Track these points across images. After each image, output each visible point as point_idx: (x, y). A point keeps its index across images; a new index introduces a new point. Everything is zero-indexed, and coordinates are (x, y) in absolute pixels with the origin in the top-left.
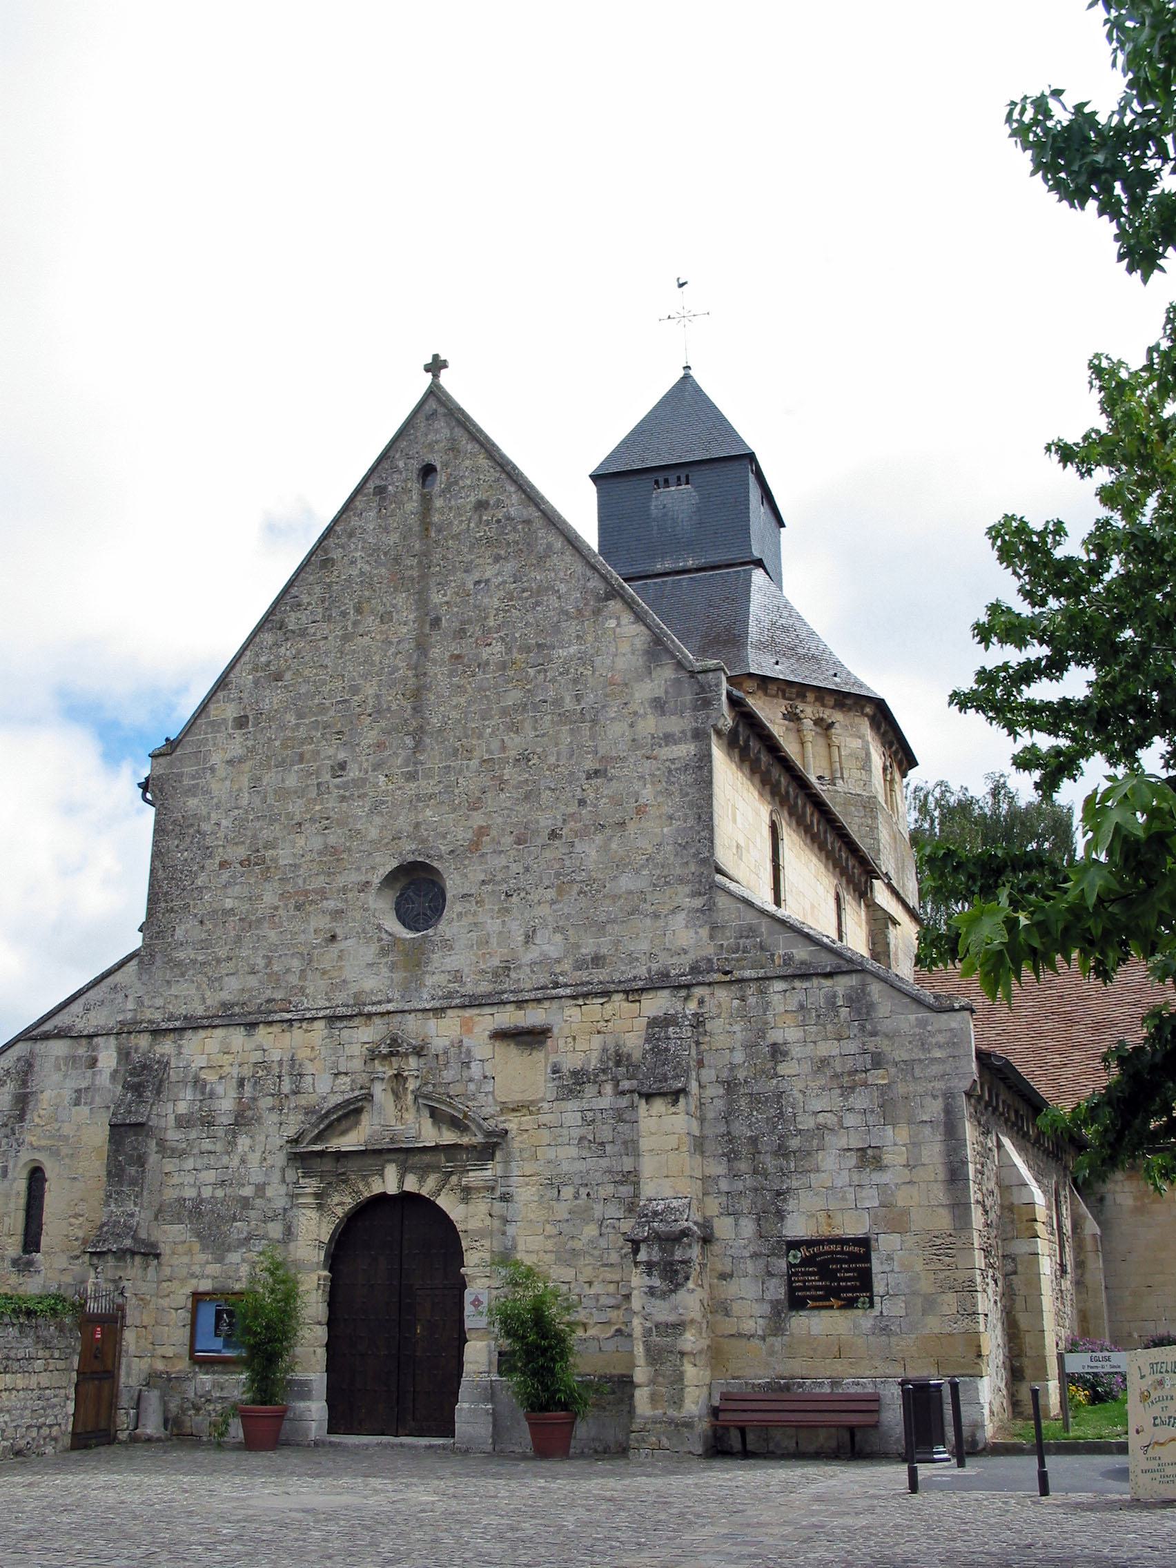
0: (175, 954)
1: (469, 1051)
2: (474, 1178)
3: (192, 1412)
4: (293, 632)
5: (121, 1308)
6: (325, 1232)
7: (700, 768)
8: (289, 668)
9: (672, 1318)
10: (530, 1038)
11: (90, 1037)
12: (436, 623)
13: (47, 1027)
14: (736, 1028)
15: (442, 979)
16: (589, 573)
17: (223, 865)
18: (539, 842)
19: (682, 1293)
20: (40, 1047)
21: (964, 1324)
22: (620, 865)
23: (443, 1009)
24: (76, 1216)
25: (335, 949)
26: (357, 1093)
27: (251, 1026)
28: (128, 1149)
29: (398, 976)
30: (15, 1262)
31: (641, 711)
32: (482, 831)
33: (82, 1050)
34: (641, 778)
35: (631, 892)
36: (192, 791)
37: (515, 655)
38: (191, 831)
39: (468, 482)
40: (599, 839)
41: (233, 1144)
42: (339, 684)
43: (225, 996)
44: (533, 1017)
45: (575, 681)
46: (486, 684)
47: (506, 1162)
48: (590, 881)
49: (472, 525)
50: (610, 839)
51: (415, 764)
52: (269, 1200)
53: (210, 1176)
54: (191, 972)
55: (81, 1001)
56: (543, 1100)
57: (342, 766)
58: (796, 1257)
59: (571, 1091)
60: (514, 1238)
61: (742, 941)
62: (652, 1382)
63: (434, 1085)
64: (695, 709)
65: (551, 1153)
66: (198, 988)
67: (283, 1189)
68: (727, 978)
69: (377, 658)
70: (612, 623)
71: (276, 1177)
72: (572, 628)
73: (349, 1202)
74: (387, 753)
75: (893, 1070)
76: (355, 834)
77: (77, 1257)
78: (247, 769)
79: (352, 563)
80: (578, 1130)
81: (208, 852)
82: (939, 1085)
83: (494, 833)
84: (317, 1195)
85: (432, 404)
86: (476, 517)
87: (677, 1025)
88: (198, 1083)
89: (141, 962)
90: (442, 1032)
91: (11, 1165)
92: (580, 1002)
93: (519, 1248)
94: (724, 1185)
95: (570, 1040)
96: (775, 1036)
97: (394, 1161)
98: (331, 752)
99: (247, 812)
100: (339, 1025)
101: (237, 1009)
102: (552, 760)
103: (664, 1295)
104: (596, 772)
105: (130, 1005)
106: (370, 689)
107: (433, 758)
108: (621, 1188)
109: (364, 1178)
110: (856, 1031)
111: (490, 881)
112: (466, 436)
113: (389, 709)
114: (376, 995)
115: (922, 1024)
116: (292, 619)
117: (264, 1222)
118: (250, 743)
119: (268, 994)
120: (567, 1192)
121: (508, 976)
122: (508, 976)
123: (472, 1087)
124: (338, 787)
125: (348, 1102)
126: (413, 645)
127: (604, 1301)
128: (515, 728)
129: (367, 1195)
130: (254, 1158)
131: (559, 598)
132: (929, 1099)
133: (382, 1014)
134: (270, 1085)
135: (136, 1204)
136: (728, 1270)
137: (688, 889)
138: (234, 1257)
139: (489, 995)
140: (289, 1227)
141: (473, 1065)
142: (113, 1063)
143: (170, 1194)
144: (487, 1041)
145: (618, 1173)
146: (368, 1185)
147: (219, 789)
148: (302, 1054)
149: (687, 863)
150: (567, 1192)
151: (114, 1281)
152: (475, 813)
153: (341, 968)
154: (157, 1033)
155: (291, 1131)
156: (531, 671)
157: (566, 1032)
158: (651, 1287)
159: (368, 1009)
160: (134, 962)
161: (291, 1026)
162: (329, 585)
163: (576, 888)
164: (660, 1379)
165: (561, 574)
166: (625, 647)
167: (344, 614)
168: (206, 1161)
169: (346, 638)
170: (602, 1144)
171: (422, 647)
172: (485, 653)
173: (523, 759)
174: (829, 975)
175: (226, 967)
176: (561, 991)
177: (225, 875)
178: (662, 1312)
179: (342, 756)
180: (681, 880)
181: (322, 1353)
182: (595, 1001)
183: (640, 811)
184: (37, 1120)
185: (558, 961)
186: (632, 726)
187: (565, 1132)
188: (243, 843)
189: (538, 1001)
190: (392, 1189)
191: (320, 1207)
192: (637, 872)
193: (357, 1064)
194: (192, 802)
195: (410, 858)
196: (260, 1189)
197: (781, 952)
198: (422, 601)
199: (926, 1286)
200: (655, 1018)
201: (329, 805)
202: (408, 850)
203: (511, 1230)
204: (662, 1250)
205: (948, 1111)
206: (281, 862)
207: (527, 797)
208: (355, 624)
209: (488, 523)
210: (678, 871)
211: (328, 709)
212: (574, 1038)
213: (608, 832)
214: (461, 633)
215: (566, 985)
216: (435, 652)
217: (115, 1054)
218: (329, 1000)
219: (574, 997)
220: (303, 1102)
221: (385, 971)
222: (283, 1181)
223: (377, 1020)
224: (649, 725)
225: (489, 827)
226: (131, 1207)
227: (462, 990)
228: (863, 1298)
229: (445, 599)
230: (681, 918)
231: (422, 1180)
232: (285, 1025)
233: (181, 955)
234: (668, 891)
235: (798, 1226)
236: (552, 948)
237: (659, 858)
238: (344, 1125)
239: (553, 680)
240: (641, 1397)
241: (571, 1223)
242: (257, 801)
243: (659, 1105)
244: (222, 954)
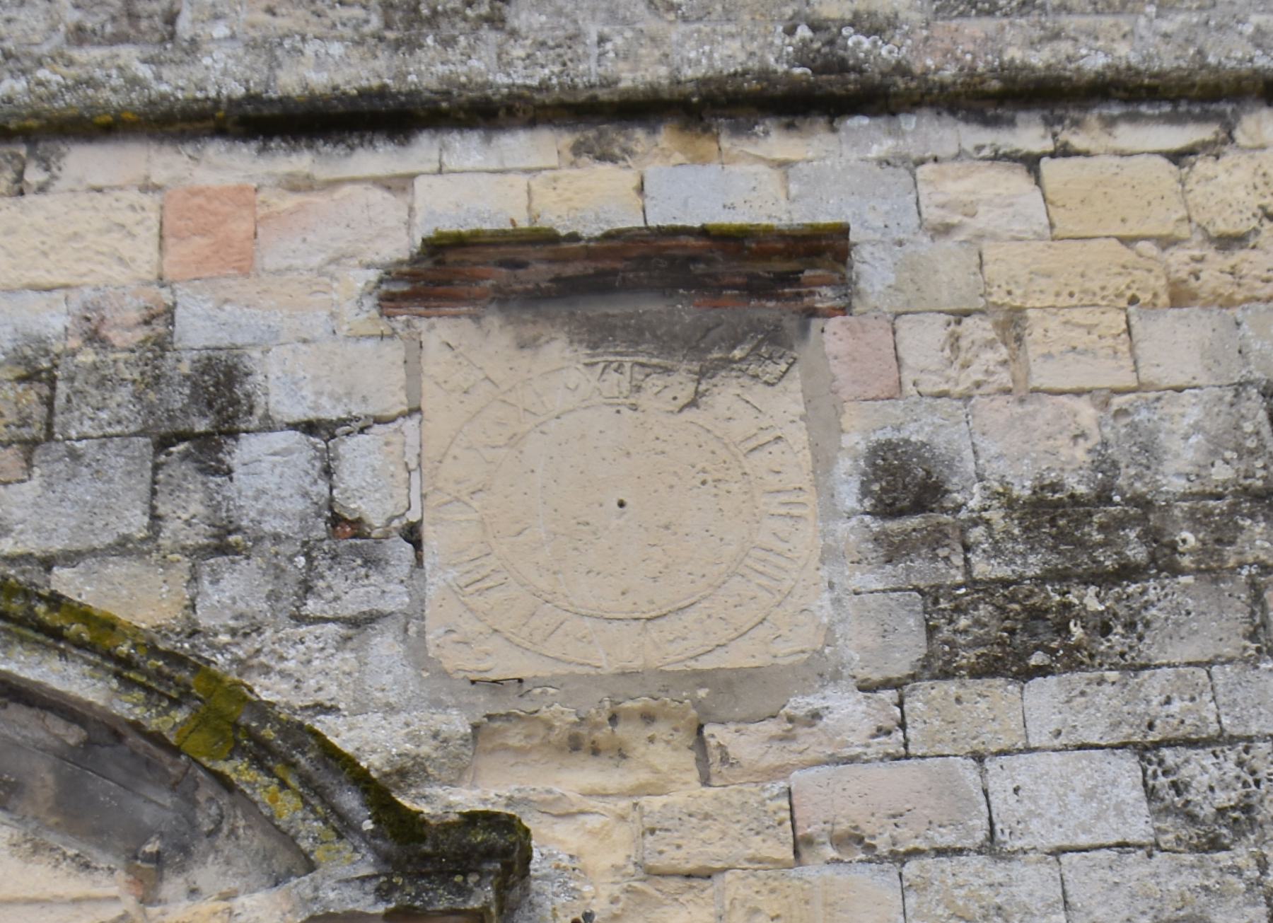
56: (821, 671)
80: (1136, 867)
92: (1029, 135)
144: (365, 316)
182: (1128, 136)
212: (1012, 324)
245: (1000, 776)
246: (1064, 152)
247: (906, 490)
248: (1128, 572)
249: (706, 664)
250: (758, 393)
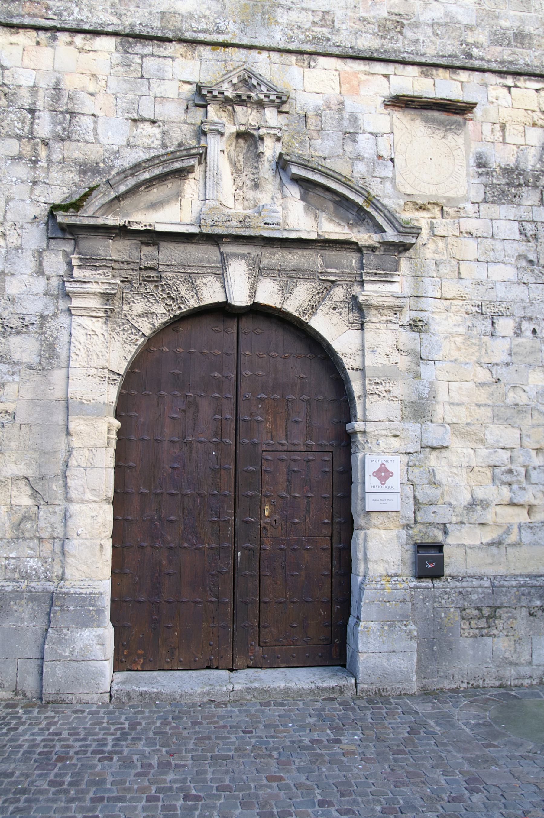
1: (354, 119)
2: (371, 292)
6: (119, 355)
15: (306, 19)
52: (12, 300)
56: (465, 199)
60: (431, 383)
67: (39, 285)
71: (26, 263)
73: (162, 313)
80: (515, 245)
84: (107, 297)
92: (509, 81)
93: (439, 398)
95: (497, 127)
97: (243, 256)
100: (139, 48)
109: (190, 279)
114: (198, 21)
120: (506, 325)
121: (401, 32)
122: (401, 32)
129: (193, 304)
140: (51, 347)
141: (361, 138)
146: (195, 289)
148: (70, 83)
150: (506, 325)
157: (493, 116)
161: (54, 38)
185: (469, 28)
190: (240, 298)
191: (109, 315)
193: (173, 111)
203: (426, 371)
212: (503, 127)
218: (119, 16)
220: (77, 155)
222: (40, 271)
227: (335, 39)
231: (286, 290)
236: (461, 11)
241: (512, 368)
245: (496, 223)
246: (516, 86)
247: (481, 163)
248: (520, 185)
249: (446, 195)
250: (456, 137)
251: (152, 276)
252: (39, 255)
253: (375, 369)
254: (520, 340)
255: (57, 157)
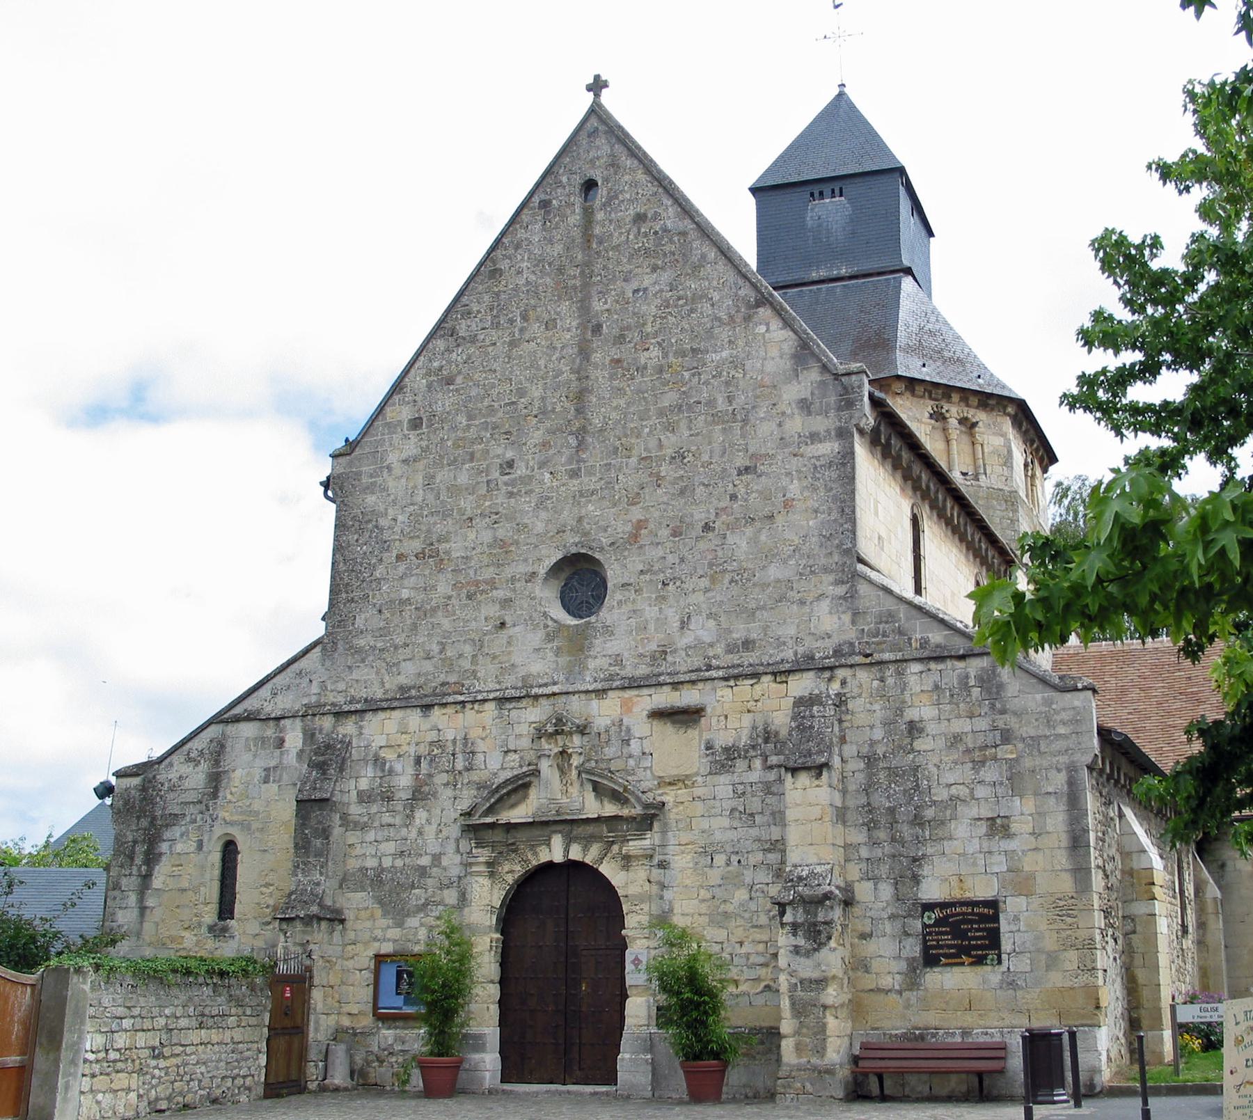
0: (355, 641)
1: (628, 730)
2: (634, 847)
3: (376, 1064)
4: (464, 338)
5: (309, 969)
6: (496, 897)
7: (843, 464)
8: (460, 373)
9: (816, 975)
10: (686, 716)
11: (277, 719)
12: (597, 329)
13: (238, 710)
14: (877, 707)
15: (602, 662)
16: (741, 282)
17: (400, 557)
18: (694, 534)
19: (824, 951)
20: (231, 729)
21: (1084, 979)
22: (770, 556)
23: (604, 691)
24: (267, 885)
25: (504, 634)
26: (525, 769)
27: (427, 708)
28: (313, 822)
29: (564, 660)
30: (211, 929)
31: (789, 412)
32: (640, 525)
33: (270, 731)
34: (788, 474)
35: (778, 581)
36: (370, 489)
37: (672, 359)
38: (370, 526)
39: (628, 196)
40: (749, 531)
41: (410, 817)
42: (507, 387)
43: (402, 680)
44: (688, 697)
45: (727, 383)
46: (643, 387)
47: (664, 833)
48: (741, 571)
49: (631, 237)
50: (760, 530)
51: (578, 462)
52: (445, 869)
53: (390, 847)
54: (371, 658)
55: (269, 686)
56: (697, 774)
57: (510, 464)
58: (931, 917)
59: (723, 766)
61: (881, 626)
62: (797, 1033)
63: (597, 762)
64: (839, 409)
65: (705, 824)
66: (377, 673)
67: (457, 859)
68: (868, 660)
69: (542, 363)
70: (762, 329)
71: (451, 848)
72: (724, 334)
74: (551, 452)
75: (1020, 746)
76: (522, 528)
77: (269, 923)
78: (421, 467)
79: (519, 273)
81: (385, 545)
82: (1063, 759)
83: (651, 526)
84: (489, 864)
85: (594, 122)
86: (635, 229)
87: (821, 704)
88: (378, 762)
89: (324, 649)
90: (603, 712)
91: (206, 838)
92: (732, 683)
94: (864, 853)
95: (722, 718)
96: (912, 714)
98: (499, 451)
99: (421, 508)
100: (508, 706)
101: (413, 692)
102: (705, 458)
103: (808, 954)
104: (747, 468)
105: (315, 689)
106: (536, 392)
107: (594, 456)
108: (769, 855)
109: (533, 847)
110: (986, 709)
111: (648, 571)
112: (626, 152)
113: (553, 410)
115: (1048, 702)
116: (463, 326)
117: (441, 889)
118: (424, 444)
119: (442, 678)
123: (631, 762)
124: (506, 484)
125: (517, 777)
126: (576, 350)
127: (753, 959)
128: (671, 428)
129: (535, 863)
130: (430, 831)
131: (713, 305)
132: (1054, 772)
133: (548, 696)
134: (444, 763)
135: (321, 874)
136: (868, 930)
137: (831, 578)
138: (413, 922)
139: (648, 677)
140: (464, 894)
141: (632, 742)
142: (300, 744)
143: (353, 864)
144: (645, 719)
145: (766, 842)
146: (536, 854)
147: (396, 486)
148: (474, 734)
149: (831, 554)
150: (720, 859)
151: (302, 945)
152: (634, 508)
153: (509, 653)
154: (339, 715)
155: (465, 805)
156: (687, 375)
158: (796, 946)
159: (535, 691)
160: (318, 649)
161: (464, 707)
162: (498, 294)
163: (728, 577)
164: (804, 1030)
165: (715, 283)
166: (774, 352)
167: (511, 321)
168: (386, 833)
169: (513, 344)
170: (752, 815)
171: (584, 352)
172: (643, 358)
173: (679, 456)
174: (962, 657)
175: (403, 653)
176: (714, 674)
177: (402, 568)
178: (806, 968)
179: (509, 454)
180: (826, 570)
181: (494, 1010)
183: (788, 504)
184: (229, 797)
185: (711, 645)
186: (780, 425)
187: (718, 804)
188: (418, 537)
189: (693, 682)
190: (558, 857)
191: (492, 875)
192: (785, 562)
193: (525, 743)
194: (371, 499)
195: (574, 550)
196: (437, 858)
197: (918, 636)
198: (584, 308)
199: (1050, 943)
200: (801, 698)
201: (499, 501)
202: (572, 543)
203: (668, 895)
204: (807, 912)
205: (1072, 783)
206: (454, 555)
207: (682, 492)
208: (522, 330)
209: (646, 235)
210: (823, 561)
211: (497, 411)
212: (726, 717)
213: (758, 524)
214: (620, 339)
215: (718, 668)
216: (596, 357)
217: (301, 735)
218: (499, 683)
219: (726, 679)
220: (476, 778)
221: (550, 655)
222: (458, 851)
223: (543, 701)
224: (797, 425)
225: (646, 520)
226: (317, 877)
227: (623, 673)
228: (992, 955)
229: (606, 307)
230: (825, 605)
231: (585, 849)
232: (459, 707)
233: (361, 642)
234: (814, 579)
235: (932, 890)
237: (805, 549)
238: (513, 798)
239: (707, 383)
240: (787, 1047)
242: (430, 497)
243: (804, 779)
244: (399, 640)
247: (709, 747)
251: (513, 848)
252: (457, 841)
253: (633, 895)
254: (730, 868)
255: (466, 781)
